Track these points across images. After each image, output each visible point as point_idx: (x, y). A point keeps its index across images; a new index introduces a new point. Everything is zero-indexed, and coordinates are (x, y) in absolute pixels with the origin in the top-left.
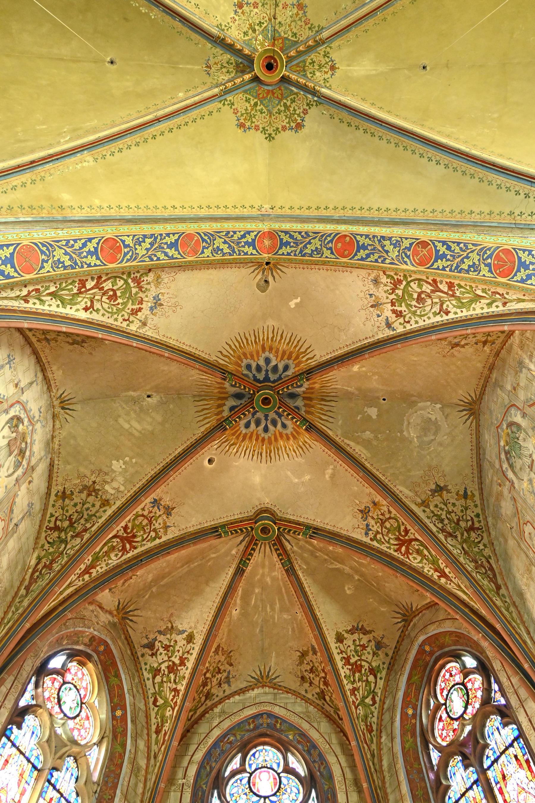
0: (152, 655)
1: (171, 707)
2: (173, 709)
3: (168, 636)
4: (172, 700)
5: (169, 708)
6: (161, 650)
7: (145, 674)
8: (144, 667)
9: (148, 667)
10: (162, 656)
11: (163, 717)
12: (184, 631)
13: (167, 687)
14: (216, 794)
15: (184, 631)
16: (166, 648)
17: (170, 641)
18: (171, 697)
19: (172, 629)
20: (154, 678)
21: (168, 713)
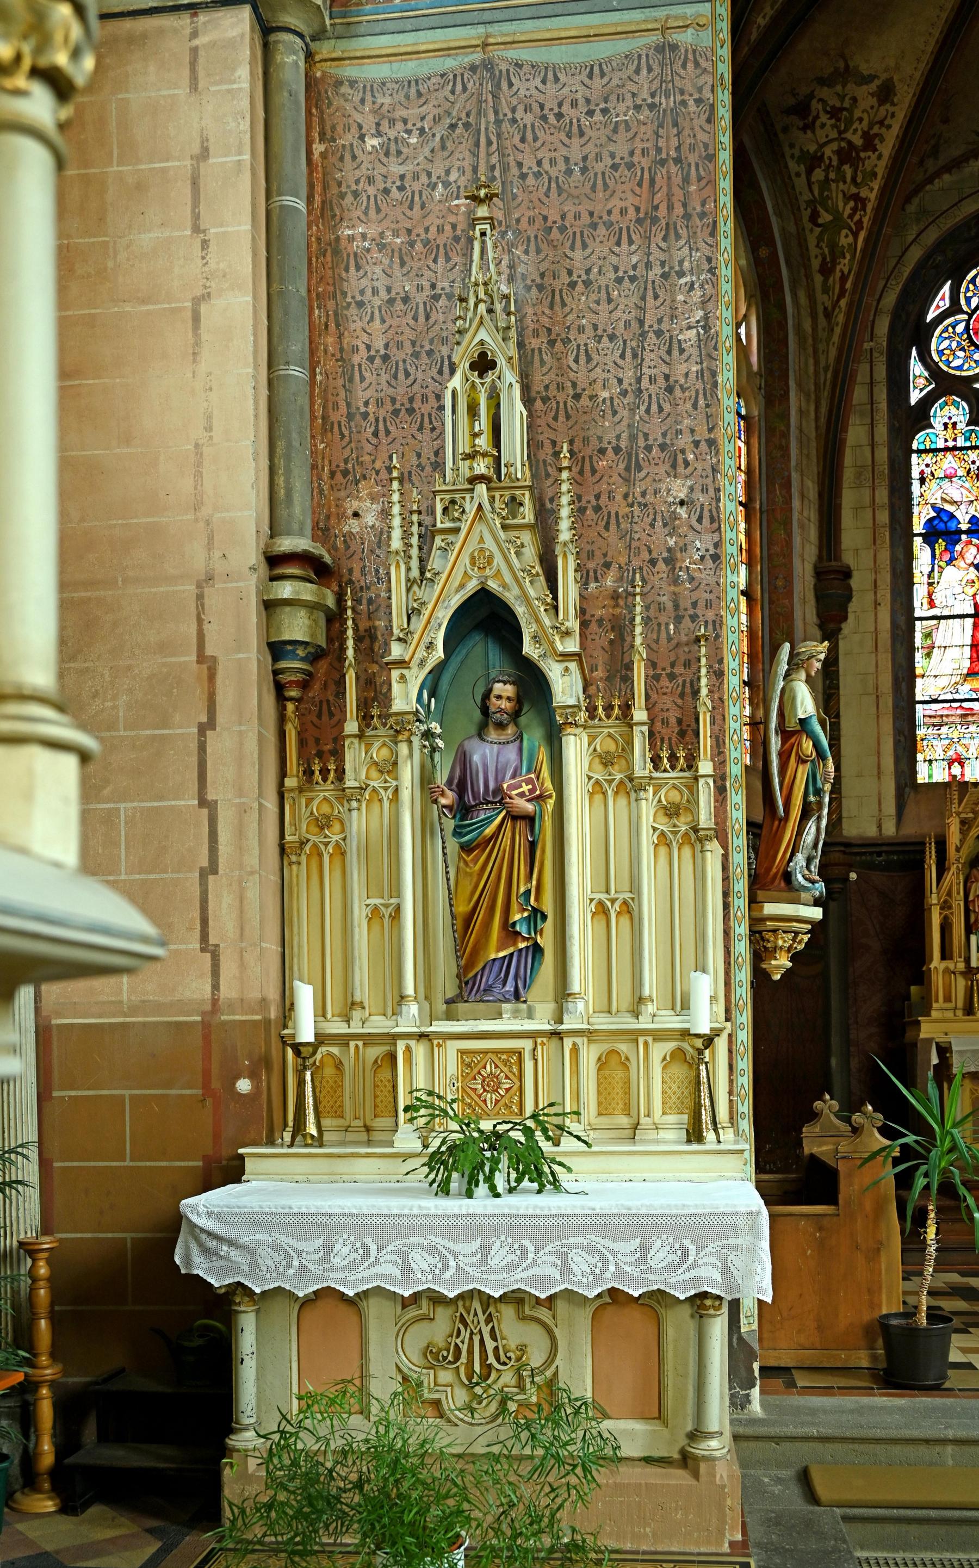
0: (805, 129)
1: (850, 229)
2: (856, 236)
3: (839, 88)
4: (851, 216)
5: (844, 232)
6: (824, 118)
7: (792, 165)
8: (788, 151)
9: (797, 152)
10: (826, 129)
11: (833, 246)
12: (871, 78)
13: (837, 192)
14: (914, 352)
15: (871, 78)
16: (834, 113)
17: (842, 98)
18: (848, 211)
19: (846, 74)
20: (809, 172)
21: (845, 240)
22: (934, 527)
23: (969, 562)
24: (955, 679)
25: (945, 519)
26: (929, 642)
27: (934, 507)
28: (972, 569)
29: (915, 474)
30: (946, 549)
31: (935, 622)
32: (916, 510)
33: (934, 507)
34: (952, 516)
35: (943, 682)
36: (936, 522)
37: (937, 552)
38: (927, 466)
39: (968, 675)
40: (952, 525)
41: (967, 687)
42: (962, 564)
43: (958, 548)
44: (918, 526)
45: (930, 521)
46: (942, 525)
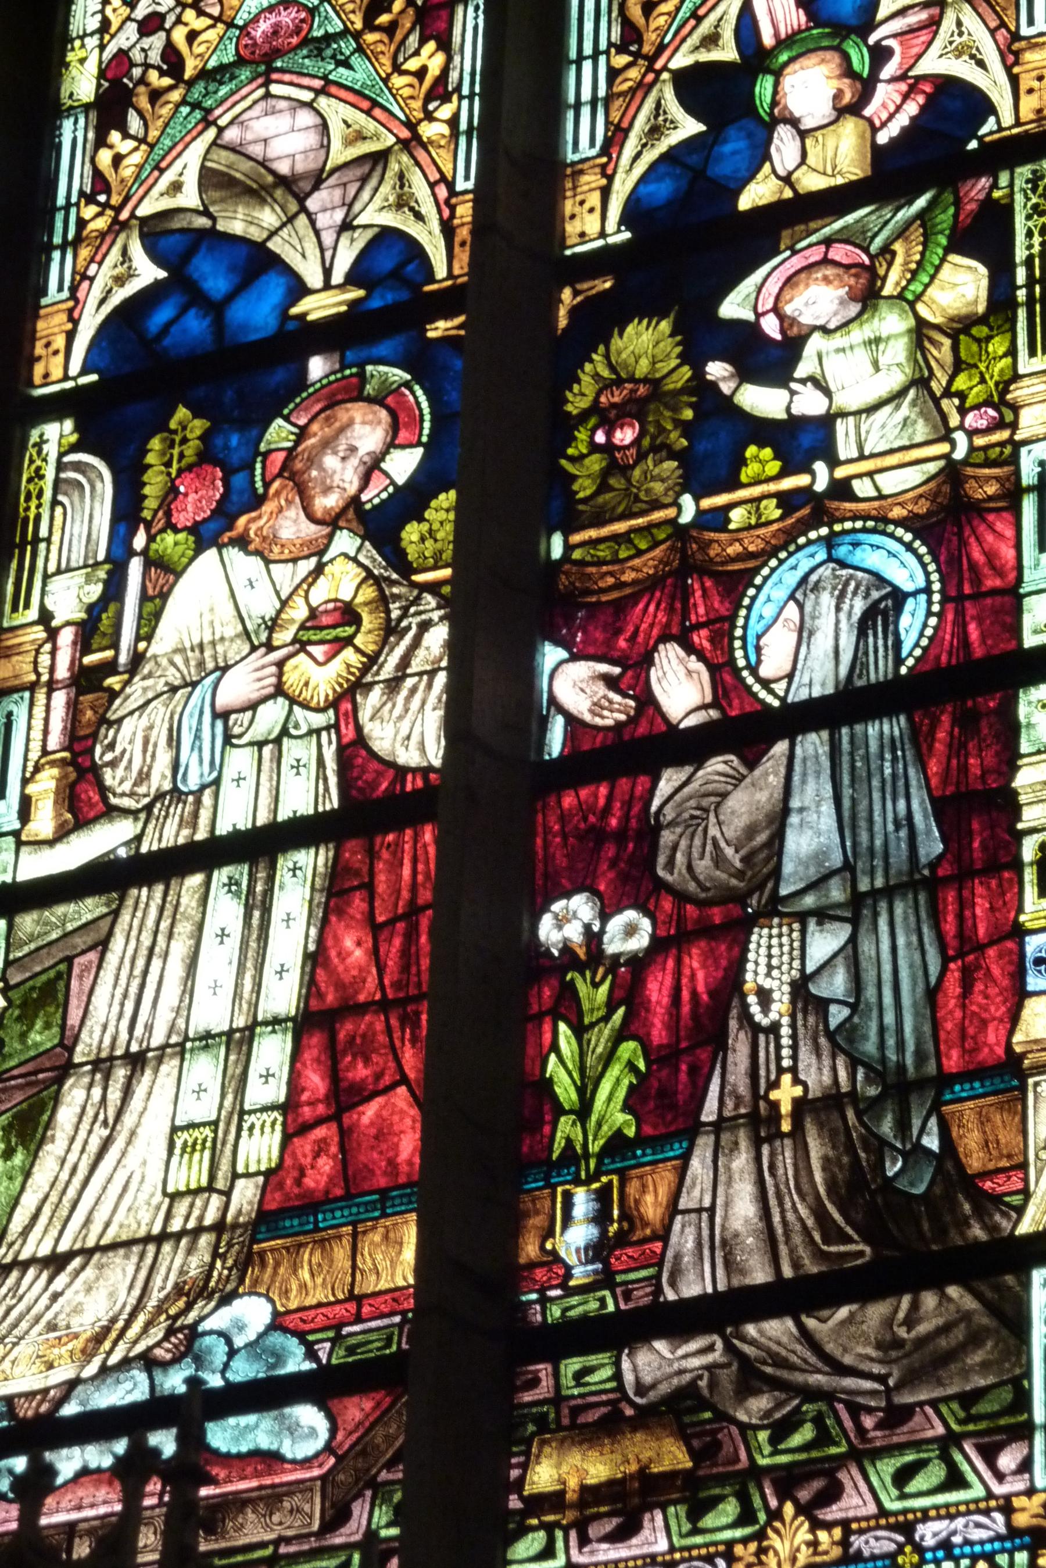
22: (150, 345)
23: (328, 502)
24: (180, 1263)
25: (217, 283)
26: (41, 1038)
27: (155, 233)
28: (345, 542)
29: (82, 82)
30: (207, 456)
31: (90, 908)
32: (58, 271)
33: (155, 233)
34: (258, 261)
35: (97, 1296)
36: (163, 315)
37: (153, 486)
38: (151, 25)
39: (266, 1221)
40: (257, 312)
41: (251, 1314)
42: (293, 526)
43: (279, 433)
44: (64, 355)
45: (127, 318)
46: (196, 325)
